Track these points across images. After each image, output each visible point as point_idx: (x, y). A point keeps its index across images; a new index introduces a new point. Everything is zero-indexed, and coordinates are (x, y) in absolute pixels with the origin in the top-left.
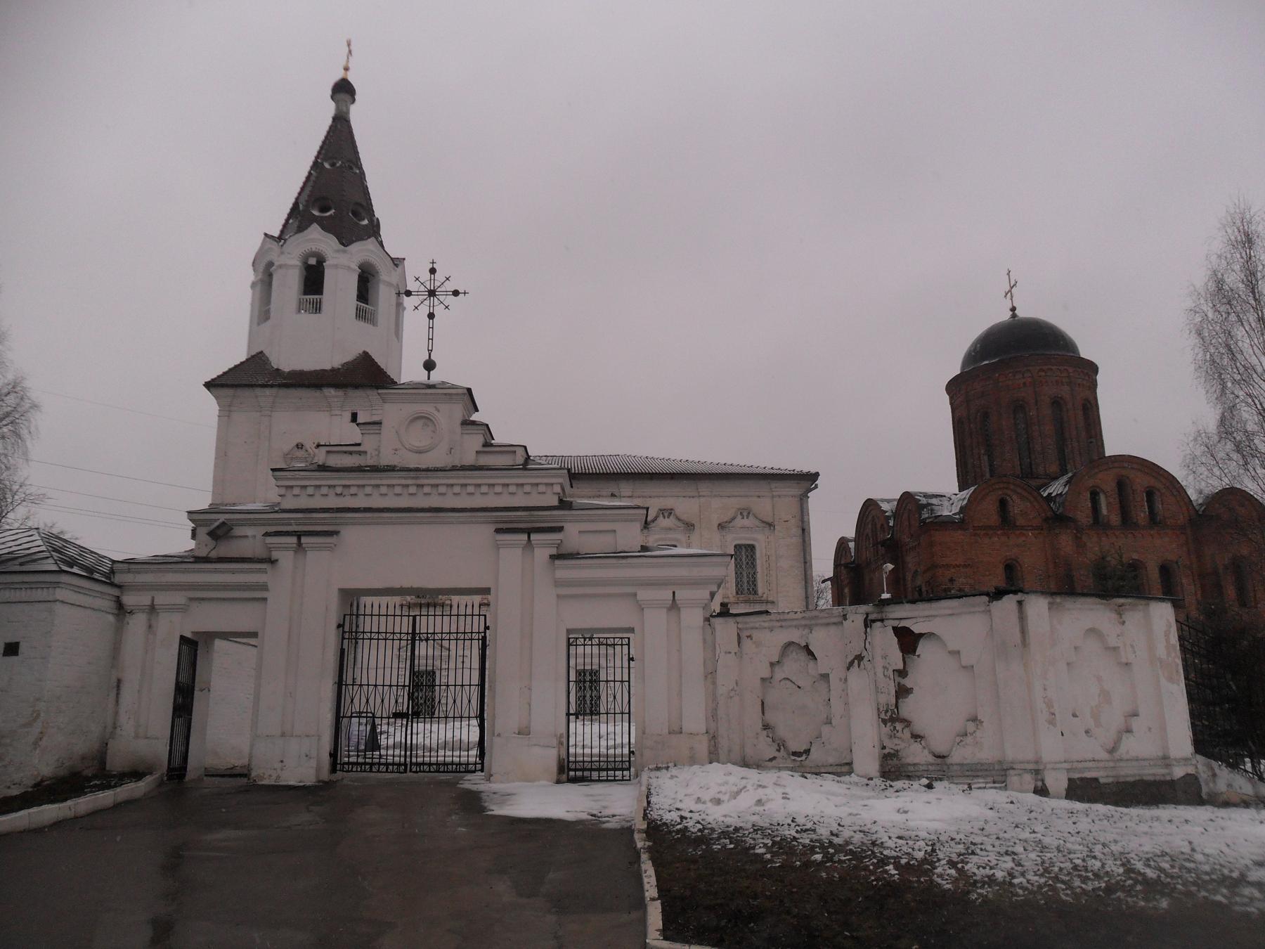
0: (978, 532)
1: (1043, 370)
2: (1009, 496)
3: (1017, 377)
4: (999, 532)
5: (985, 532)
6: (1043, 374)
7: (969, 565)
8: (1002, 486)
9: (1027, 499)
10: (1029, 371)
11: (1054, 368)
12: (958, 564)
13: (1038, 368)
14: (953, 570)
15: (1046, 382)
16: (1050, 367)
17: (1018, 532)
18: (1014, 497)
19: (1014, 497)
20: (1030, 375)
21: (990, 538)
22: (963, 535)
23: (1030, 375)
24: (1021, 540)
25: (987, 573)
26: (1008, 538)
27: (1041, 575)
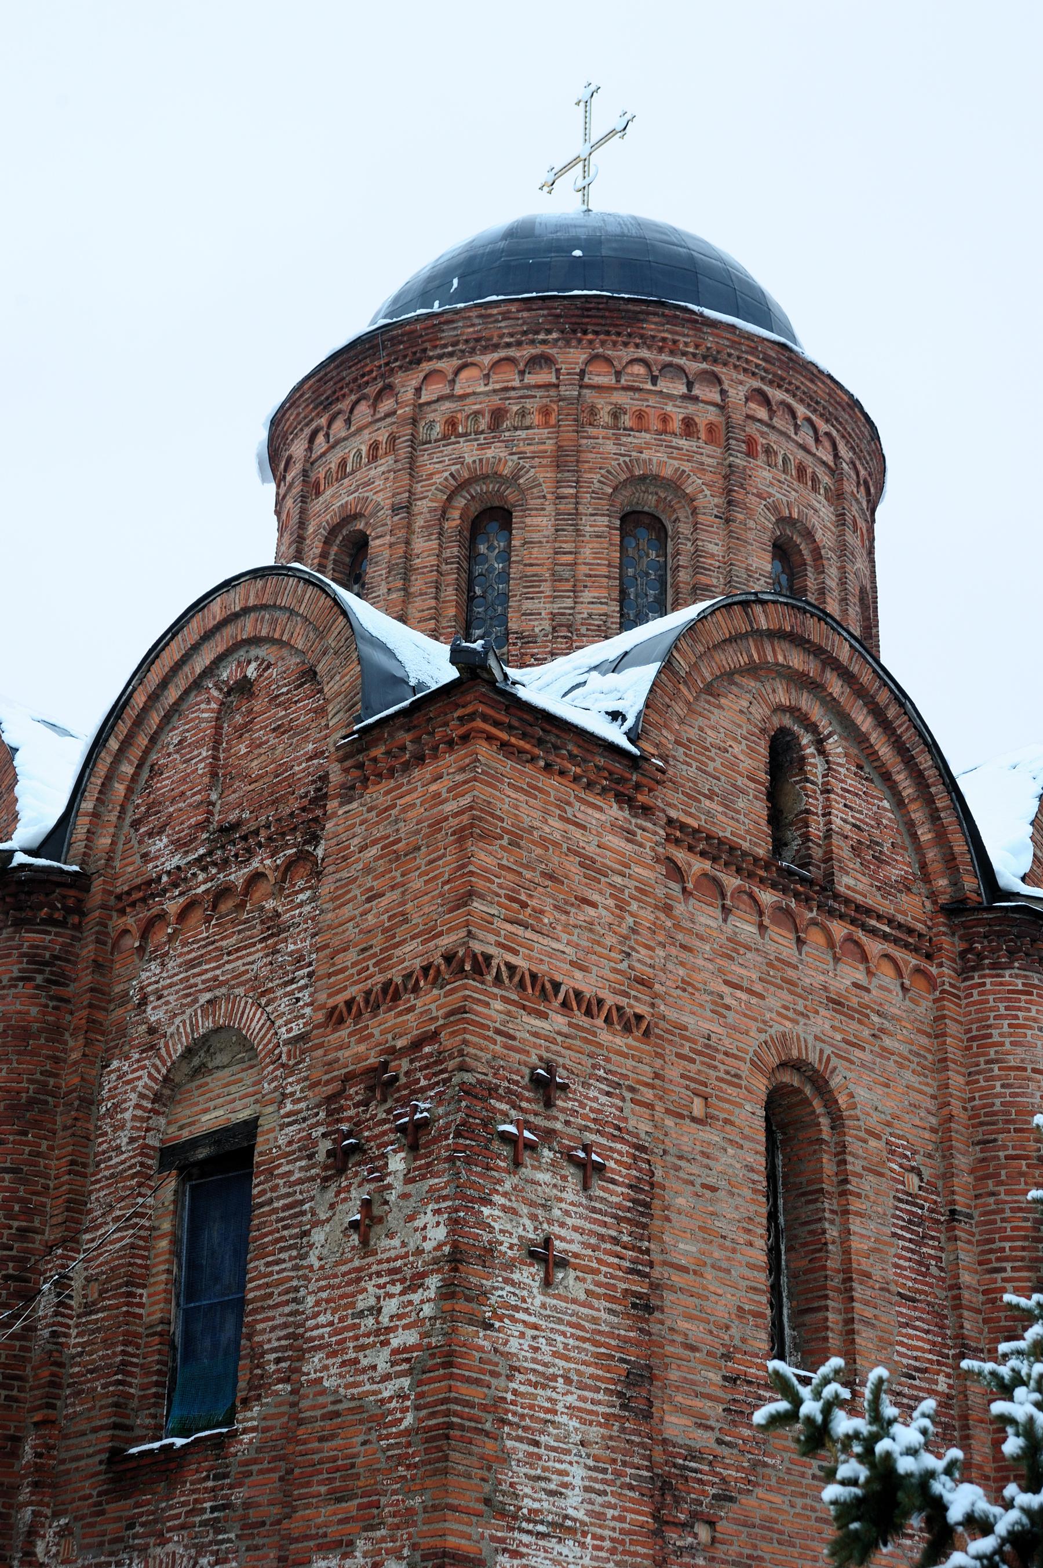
0: (680, 855)
1: (766, 401)
2: (812, 728)
3: (663, 385)
4: (767, 897)
5: (707, 865)
6: (762, 413)
7: (639, 1018)
8: (797, 660)
9: (886, 777)
10: (715, 379)
11: (801, 410)
12: (588, 992)
13: (757, 384)
14: (559, 1021)
15: (768, 451)
16: (790, 400)
17: (839, 929)
18: (835, 746)
19: (835, 746)
20: (717, 398)
21: (726, 911)
22: (630, 836)
23: (717, 398)
24: (851, 973)
25: (698, 1108)
26: (800, 942)
27: (912, 1199)
